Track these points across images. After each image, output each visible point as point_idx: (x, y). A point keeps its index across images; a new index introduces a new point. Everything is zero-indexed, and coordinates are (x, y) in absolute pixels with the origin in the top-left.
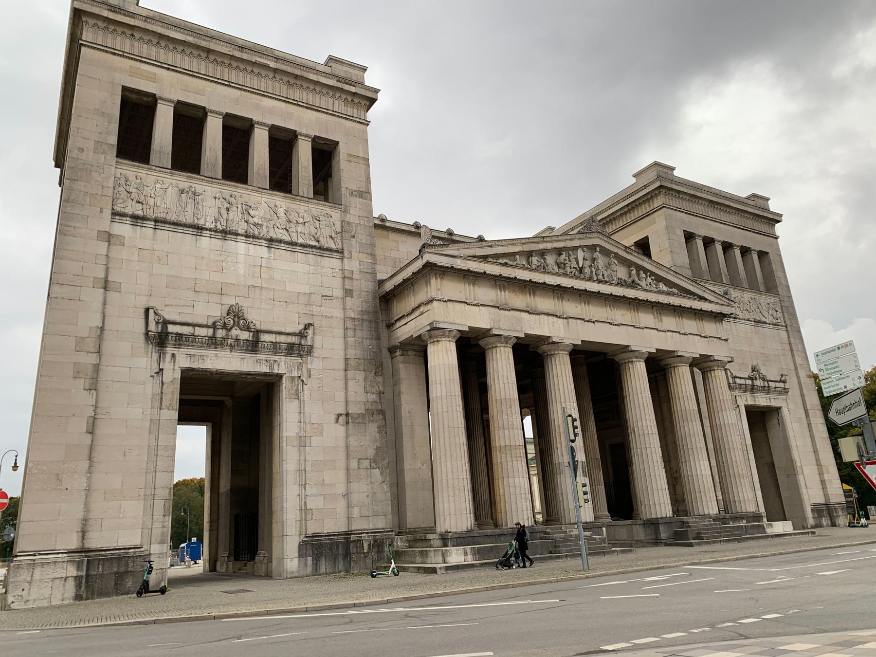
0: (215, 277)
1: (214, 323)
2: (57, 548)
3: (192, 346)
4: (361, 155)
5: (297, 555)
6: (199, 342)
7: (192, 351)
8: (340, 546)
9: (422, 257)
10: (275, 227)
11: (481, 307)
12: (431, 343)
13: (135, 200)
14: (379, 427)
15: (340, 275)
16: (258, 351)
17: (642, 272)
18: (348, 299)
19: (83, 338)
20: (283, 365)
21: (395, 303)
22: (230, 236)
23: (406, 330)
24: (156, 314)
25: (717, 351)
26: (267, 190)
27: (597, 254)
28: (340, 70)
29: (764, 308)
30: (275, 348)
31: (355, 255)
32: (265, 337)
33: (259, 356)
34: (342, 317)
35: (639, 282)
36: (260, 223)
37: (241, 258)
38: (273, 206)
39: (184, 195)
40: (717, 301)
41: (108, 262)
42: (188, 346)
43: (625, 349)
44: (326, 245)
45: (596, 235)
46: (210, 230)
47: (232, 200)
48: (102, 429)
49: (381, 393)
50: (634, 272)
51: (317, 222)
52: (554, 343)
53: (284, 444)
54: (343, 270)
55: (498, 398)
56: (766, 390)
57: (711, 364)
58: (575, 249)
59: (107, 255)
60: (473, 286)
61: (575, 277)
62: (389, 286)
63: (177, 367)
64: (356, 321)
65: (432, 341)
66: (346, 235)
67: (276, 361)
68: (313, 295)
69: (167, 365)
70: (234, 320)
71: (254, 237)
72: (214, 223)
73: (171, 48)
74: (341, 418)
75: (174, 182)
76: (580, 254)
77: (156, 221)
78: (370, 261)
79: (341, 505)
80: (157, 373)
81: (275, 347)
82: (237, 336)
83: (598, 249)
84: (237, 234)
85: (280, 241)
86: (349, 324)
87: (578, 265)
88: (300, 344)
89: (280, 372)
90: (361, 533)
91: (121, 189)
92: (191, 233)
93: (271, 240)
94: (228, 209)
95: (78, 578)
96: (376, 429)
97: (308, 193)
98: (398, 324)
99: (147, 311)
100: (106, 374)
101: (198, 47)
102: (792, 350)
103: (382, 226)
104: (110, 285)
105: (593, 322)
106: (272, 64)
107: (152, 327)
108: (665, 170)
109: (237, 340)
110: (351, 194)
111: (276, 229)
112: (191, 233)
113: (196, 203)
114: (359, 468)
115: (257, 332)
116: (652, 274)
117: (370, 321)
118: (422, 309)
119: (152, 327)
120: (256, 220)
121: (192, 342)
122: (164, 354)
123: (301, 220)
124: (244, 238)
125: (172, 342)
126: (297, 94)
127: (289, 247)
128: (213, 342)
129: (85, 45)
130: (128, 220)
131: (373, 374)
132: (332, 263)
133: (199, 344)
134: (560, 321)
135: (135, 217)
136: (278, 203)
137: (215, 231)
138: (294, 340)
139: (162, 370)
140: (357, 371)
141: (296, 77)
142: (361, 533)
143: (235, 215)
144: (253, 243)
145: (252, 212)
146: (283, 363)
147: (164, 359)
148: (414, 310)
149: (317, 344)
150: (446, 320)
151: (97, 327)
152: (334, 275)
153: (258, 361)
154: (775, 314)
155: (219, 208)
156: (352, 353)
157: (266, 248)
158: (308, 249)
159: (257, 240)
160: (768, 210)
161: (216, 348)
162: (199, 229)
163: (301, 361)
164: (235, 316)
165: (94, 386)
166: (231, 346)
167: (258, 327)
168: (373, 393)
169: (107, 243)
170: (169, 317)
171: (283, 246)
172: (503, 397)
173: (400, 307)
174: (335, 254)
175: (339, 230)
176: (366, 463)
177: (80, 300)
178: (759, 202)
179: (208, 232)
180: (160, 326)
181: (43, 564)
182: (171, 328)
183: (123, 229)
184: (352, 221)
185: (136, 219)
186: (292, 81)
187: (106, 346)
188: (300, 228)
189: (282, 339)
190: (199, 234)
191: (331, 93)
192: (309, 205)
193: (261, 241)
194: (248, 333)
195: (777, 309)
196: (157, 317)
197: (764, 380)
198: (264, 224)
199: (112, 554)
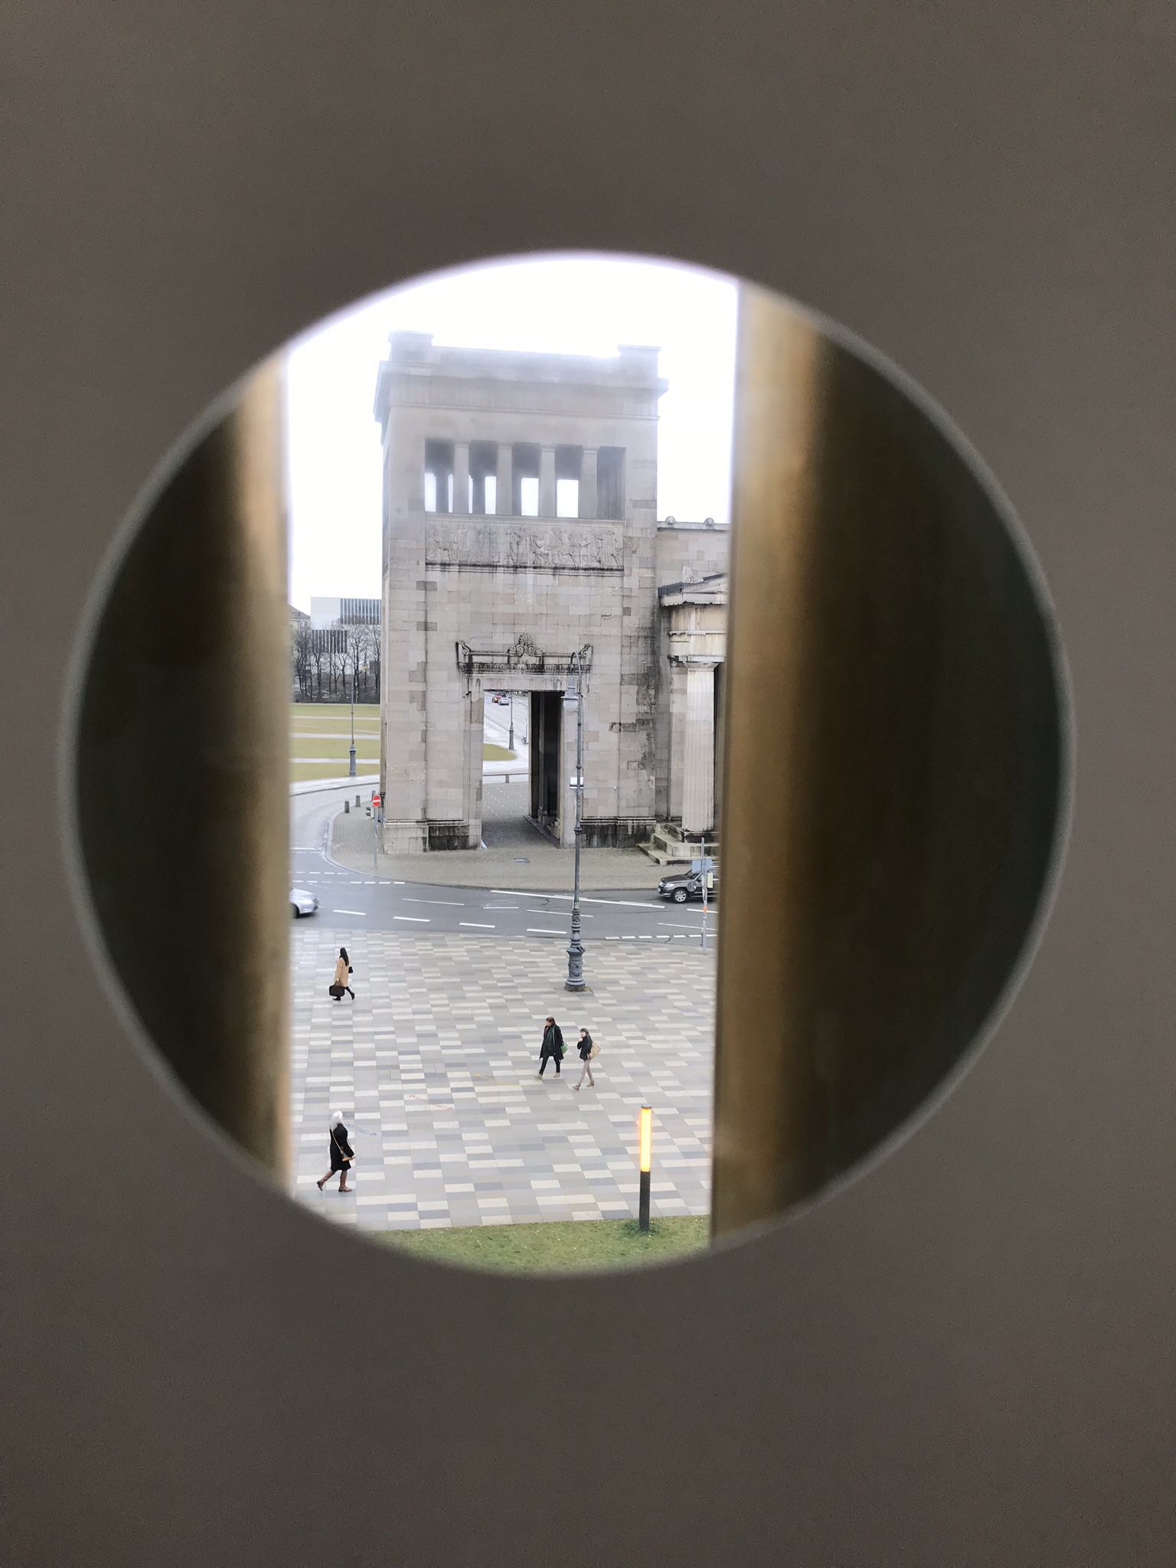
0: (508, 609)
2: (410, 818)
7: (492, 675)
12: (691, 671)
18: (626, 617)
19: (413, 671)
20: (563, 683)
31: (635, 571)
32: (550, 662)
33: (546, 676)
34: (620, 634)
36: (546, 552)
37: (530, 589)
41: (426, 606)
46: (503, 566)
47: (522, 533)
48: (431, 739)
51: (600, 541)
53: (566, 749)
54: (622, 588)
62: (669, 601)
63: (481, 690)
64: (632, 638)
68: (593, 617)
79: (613, 797)
80: (467, 694)
81: (558, 668)
86: (626, 643)
89: (562, 690)
93: (555, 568)
95: (424, 839)
96: (646, 737)
99: (457, 644)
100: (432, 697)
104: (429, 625)
107: (461, 659)
110: (635, 506)
113: (491, 542)
117: (646, 637)
119: (461, 659)
123: (584, 543)
124: (532, 569)
127: (573, 572)
131: (645, 687)
132: (611, 581)
135: (443, 565)
137: (507, 567)
139: (470, 692)
143: (524, 547)
145: (539, 543)
146: (565, 681)
149: (595, 663)
150: (702, 654)
151: (422, 662)
152: (614, 593)
153: (544, 681)
155: (511, 543)
165: (424, 707)
176: (635, 765)
179: (503, 569)
180: (467, 657)
181: (402, 828)
183: (435, 575)
184: (635, 535)
188: (583, 551)
192: (593, 525)
193: (547, 570)
198: (550, 552)
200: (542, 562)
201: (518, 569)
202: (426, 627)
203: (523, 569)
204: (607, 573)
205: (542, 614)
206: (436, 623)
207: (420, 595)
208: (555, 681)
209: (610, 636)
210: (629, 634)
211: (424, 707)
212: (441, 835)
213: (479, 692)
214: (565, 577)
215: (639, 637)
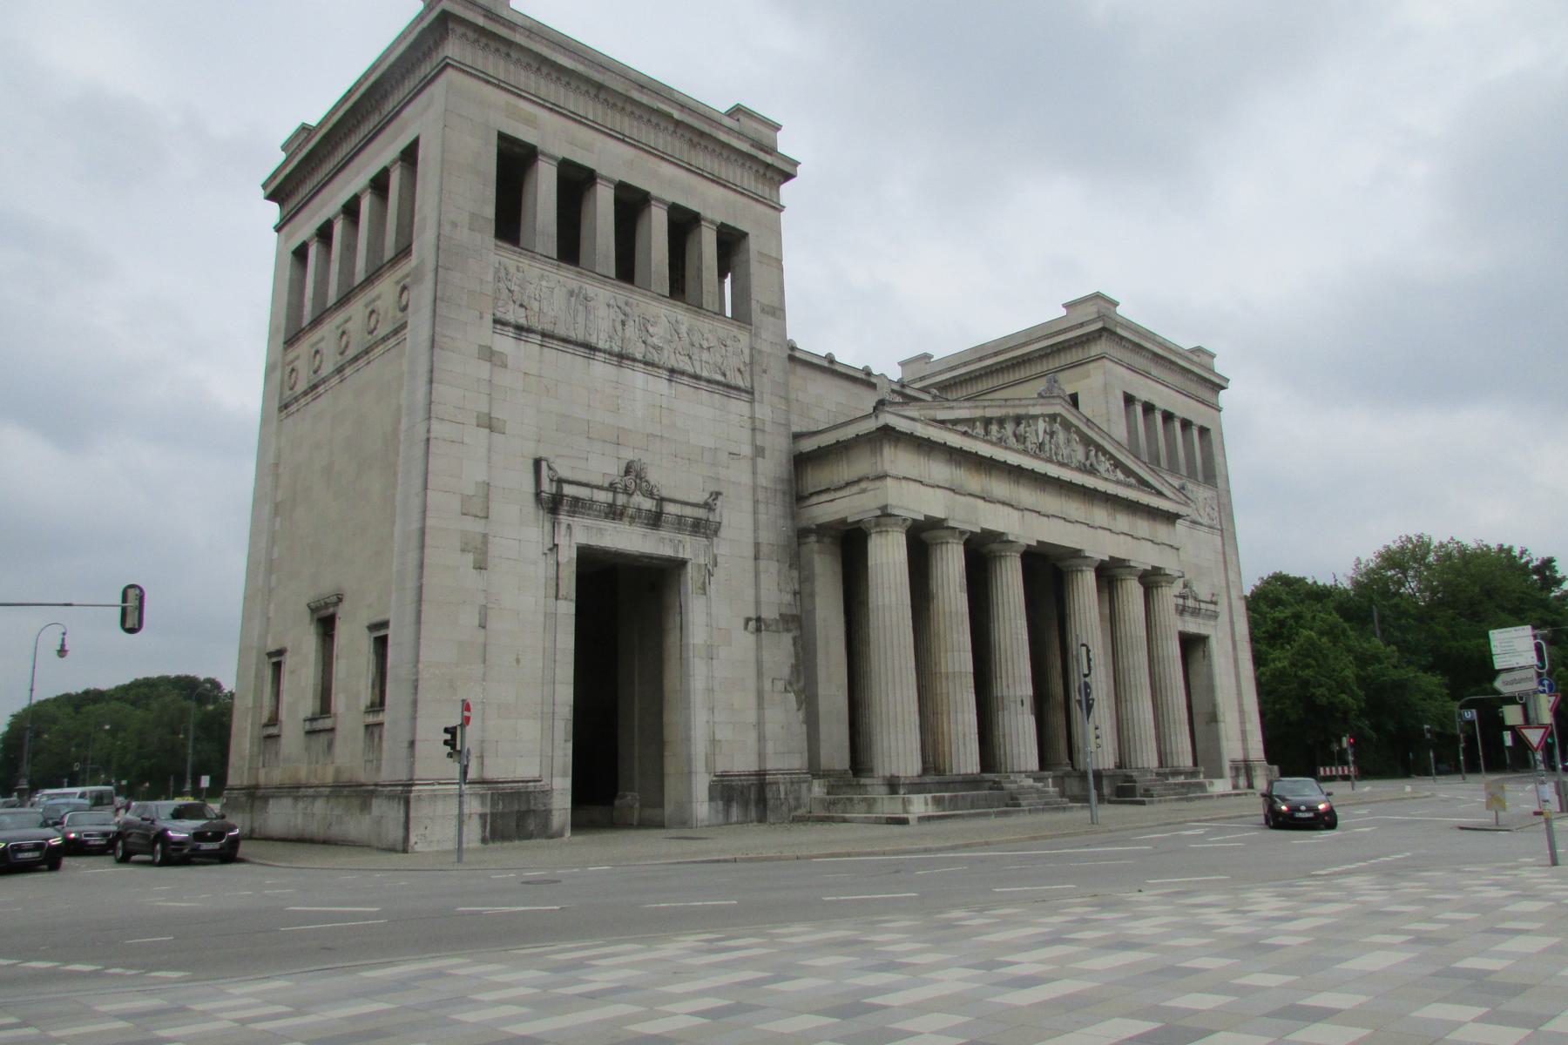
1: (611, 484)
3: (588, 515)
4: (774, 255)
5: (707, 799)
6: (596, 510)
7: (588, 522)
8: (753, 789)
9: (877, 417)
10: (677, 352)
11: (937, 489)
12: (877, 532)
13: (518, 303)
14: (795, 639)
15: (748, 424)
16: (659, 526)
17: (1100, 454)
18: (759, 460)
19: (470, 497)
20: (688, 548)
21: (809, 470)
22: (627, 362)
23: (830, 510)
24: (550, 468)
25: (1169, 563)
26: (553, 259)
27: (1057, 426)
28: (749, 126)
29: (1201, 504)
30: (679, 524)
32: (670, 508)
33: (663, 533)
35: (1098, 467)
36: (661, 345)
38: (673, 321)
39: (573, 299)
40: (1174, 498)
42: (583, 514)
43: (1076, 554)
44: (733, 382)
45: (1058, 401)
46: (605, 352)
47: (627, 309)
49: (795, 594)
50: (1093, 453)
51: (723, 347)
52: (1130, 567)
55: (947, 610)
56: (1196, 612)
57: (1159, 578)
58: (1035, 417)
59: (490, 381)
60: (929, 460)
61: (1035, 456)
62: (808, 445)
65: (878, 530)
66: (757, 369)
67: (680, 541)
69: (562, 540)
70: (635, 482)
71: (653, 365)
72: (608, 343)
73: (564, 83)
74: (750, 623)
75: (562, 279)
76: (1041, 425)
77: (544, 335)
78: (784, 408)
80: (551, 550)
82: (639, 503)
83: (1059, 420)
84: (634, 360)
85: (683, 373)
86: (761, 496)
87: (1038, 438)
88: (707, 520)
89: (686, 556)
90: (776, 774)
91: (501, 285)
92: (582, 354)
93: (672, 371)
94: (623, 323)
96: (791, 642)
97: (713, 304)
98: (815, 500)
101: (588, 80)
102: (1225, 562)
103: (795, 359)
105: (1048, 516)
106: (676, 115)
108: (1107, 305)
109: (639, 510)
110: (763, 310)
111: (678, 355)
112: (582, 354)
114: (773, 691)
115: (662, 500)
116: (1112, 457)
118: (863, 485)
120: (655, 340)
121: (589, 509)
122: (559, 523)
123: (705, 345)
124: (642, 366)
125: (566, 508)
126: (701, 160)
127: (692, 382)
128: (614, 513)
129: (453, 66)
130: (511, 331)
131: (787, 565)
132: (739, 407)
133: (596, 513)
134: (1016, 514)
135: (519, 328)
136: (679, 317)
138: (701, 513)
140: (770, 562)
141: (702, 134)
142: (776, 774)
143: (631, 331)
144: (653, 373)
145: (651, 329)
146: (689, 544)
147: (559, 528)
148: (848, 484)
149: (725, 523)
151: (484, 482)
153: (662, 540)
154: (1211, 512)
155: (613, 320)
156: (765, 537)
157: (666, 381)
158: (713, 386)
159: (656, 369)
160: (1212, 371)
161: (614, 519)
162: (591, 348)
163: (707, 543)
164: (636, 477)
166: (631, 517)
167: (665, 493)
168: (788, 593)
169: (488, 364)
170: (564, 472)
171: (686, 380)
172: (954, 610)
173: (817, 478)
174: (744, 394)
175: (747, 361)
176: (780, 685)
177: (463, 443)
178: (1204, 359)
179: (603, 355)
180: (554, 484)
181: (445, 796)
182: (568, 490)
183: (505, 343)
184: (764, 349)
185: (521, 330)
186: (696, 139)
187: (495, 507)
188: (705, 356)
189: (688, 511)
190: (592, 357)
191: (740, 161)
192: (715, 323)
193: (660, 371)
194: (651, 501)
195: (1214, 506)
196: (551, 472)
197: (1196, 599)
198: (666, 347)
199: (512, 788)
200: (655, 357)
201: (624, 361)
202: (489, 424)
203: (629, 363)
204: (734, 393)
205: (653, 435)
206: (505, 422)
207: (484, 369)
208: (676, 542)
209: (740, 484)
210: (764, 485)
211: (480, 566)
212: (506, 810)
213: (570, 546)
214: (683, 389)
215: (776, 490)
